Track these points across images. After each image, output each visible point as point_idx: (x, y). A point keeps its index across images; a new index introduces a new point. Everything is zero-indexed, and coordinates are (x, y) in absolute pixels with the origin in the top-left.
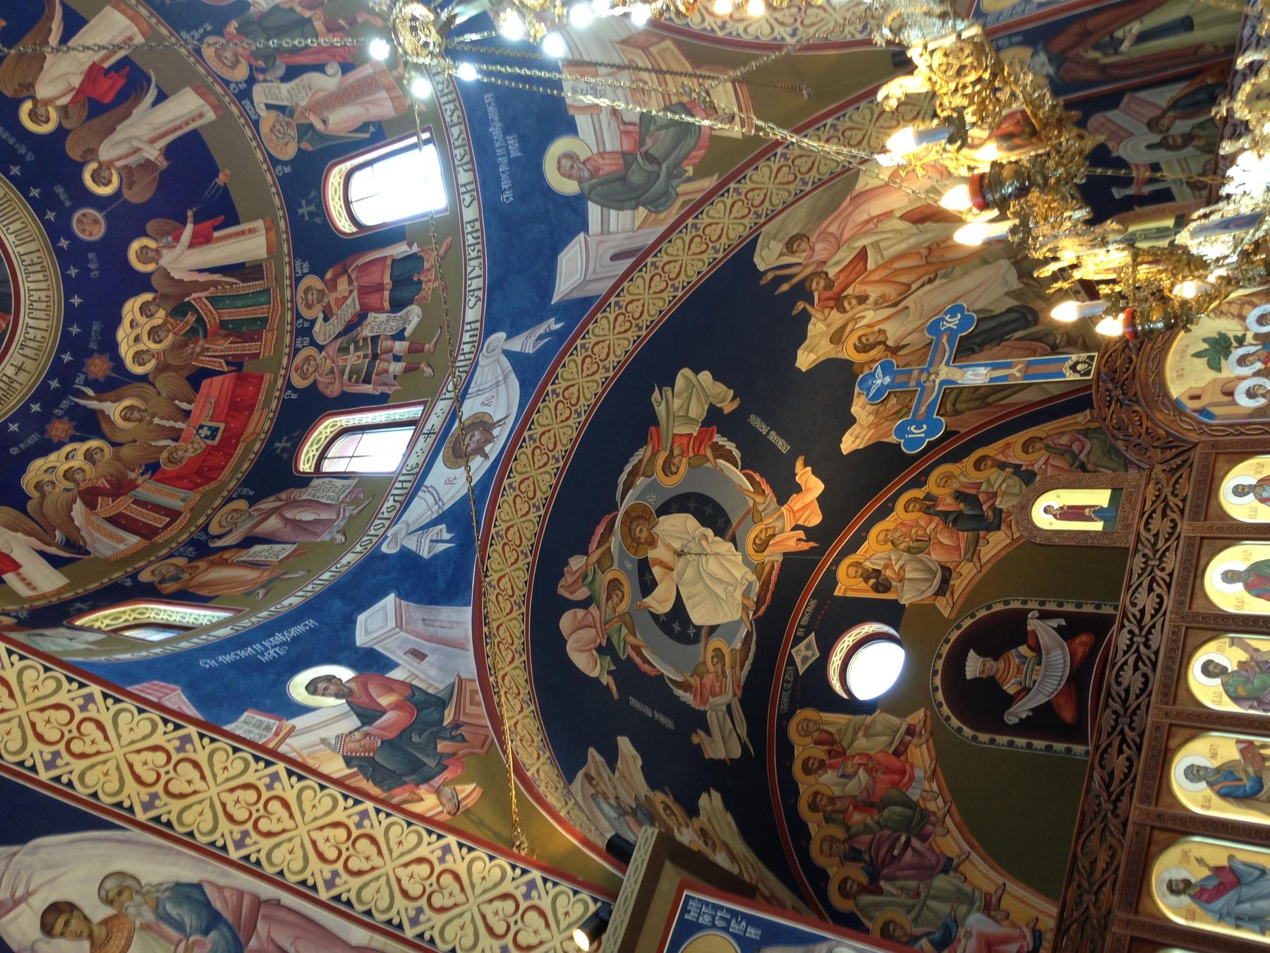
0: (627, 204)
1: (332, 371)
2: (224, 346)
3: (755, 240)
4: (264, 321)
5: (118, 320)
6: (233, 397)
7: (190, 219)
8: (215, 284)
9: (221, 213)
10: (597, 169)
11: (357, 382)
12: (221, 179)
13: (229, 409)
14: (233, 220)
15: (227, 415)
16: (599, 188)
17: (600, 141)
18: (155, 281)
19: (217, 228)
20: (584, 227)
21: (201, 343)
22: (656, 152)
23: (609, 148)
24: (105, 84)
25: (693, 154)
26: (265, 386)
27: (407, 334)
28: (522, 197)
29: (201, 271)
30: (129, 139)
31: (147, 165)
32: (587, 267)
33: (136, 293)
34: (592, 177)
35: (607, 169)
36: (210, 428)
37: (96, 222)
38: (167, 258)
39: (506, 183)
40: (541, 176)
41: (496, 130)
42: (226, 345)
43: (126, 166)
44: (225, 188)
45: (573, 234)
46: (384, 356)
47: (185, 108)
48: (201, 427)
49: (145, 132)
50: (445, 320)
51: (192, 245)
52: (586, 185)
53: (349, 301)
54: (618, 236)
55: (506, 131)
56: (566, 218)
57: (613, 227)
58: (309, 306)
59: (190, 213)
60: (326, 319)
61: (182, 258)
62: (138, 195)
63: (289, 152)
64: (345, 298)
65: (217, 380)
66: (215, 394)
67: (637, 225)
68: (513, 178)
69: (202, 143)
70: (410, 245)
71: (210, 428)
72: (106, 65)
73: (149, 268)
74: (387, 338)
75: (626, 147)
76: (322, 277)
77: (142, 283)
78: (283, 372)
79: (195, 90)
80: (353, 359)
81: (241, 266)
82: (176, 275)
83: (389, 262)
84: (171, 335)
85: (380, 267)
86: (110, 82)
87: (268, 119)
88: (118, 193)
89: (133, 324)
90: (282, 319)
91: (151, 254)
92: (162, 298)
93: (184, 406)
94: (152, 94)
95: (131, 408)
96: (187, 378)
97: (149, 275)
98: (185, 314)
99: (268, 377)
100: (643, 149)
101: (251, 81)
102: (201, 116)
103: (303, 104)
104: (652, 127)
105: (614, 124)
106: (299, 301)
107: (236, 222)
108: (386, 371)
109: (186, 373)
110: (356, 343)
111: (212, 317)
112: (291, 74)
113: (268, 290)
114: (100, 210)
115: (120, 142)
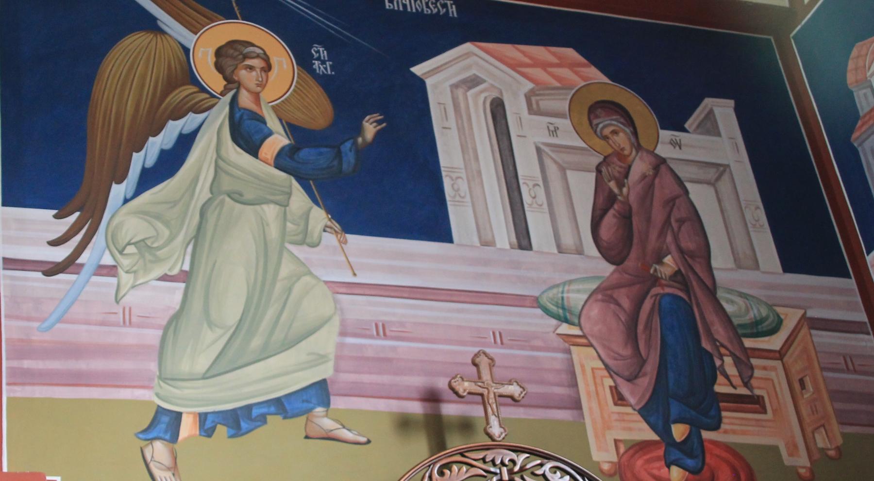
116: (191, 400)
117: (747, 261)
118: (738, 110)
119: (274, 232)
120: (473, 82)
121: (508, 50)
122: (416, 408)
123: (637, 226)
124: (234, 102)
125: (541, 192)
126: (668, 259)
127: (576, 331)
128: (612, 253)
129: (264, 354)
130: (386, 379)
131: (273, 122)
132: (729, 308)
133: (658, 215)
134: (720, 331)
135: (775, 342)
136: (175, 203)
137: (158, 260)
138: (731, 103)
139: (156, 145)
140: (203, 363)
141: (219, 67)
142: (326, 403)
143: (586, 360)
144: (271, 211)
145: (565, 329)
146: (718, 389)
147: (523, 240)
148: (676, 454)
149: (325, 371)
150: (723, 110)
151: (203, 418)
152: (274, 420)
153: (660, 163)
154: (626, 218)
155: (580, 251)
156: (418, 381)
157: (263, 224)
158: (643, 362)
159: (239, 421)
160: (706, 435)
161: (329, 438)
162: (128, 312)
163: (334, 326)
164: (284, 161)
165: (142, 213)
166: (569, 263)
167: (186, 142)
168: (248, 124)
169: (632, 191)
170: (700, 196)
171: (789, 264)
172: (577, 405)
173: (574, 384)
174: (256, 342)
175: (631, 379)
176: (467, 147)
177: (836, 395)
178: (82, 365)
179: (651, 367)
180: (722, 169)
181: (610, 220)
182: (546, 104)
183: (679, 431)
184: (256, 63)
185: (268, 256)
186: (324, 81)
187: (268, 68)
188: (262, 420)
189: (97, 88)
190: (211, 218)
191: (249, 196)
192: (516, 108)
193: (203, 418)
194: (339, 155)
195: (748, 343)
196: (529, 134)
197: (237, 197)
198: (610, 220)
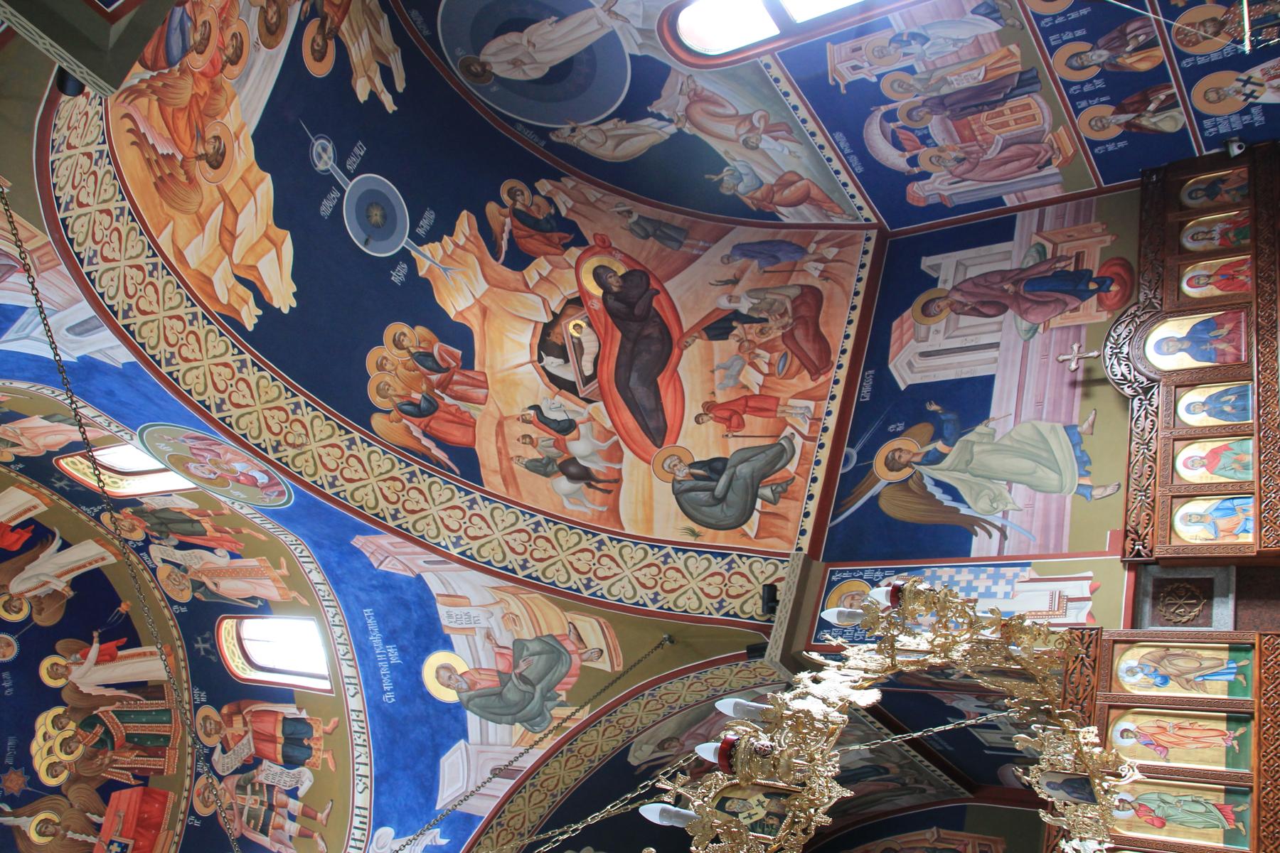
0: (505, 718)
1: (231, 807)
2: (130, 758)
3: (628, 749)
4: (167, 738)
5: (32, 734)
6: (141, 812)
7: (96, 639)
8: (120, 699)
9: (124, 635)
10: (475, 683)
11: (255, 828)
12: (123, 608)
13: (137, 825)
14: (134, 642)
15: (136, 831)
16: (477, 700)
17: (476, 658)
18: (65, 696)
19: (120, 648)
20: (464, 734)
21: (109, 754)
22: (531, 675)
23: (484, 666)
24: (15, 536)
25: (566, 680)
26: (170, 805)
27: (301, 793)
28: (404, 699)
29: (107, 686)
30: (38, 575)
31: (55, 594)
32: (469, 770)
33: (48, 708)
34: (470, 689)
35: (484, 684)
36: (120, 844)
37: (9, 645)
38: (76, 674)
39: (387, 685)
40: (420, 684)
41: (376, 639)
42: (133, 758)
43: (35, 596)
44: (127, 616)
45: (455, 740)
46: (279, 810)
47: (87, 554)
48: (112, 842)
49: (52, 570)
50: (334, 786)
51: (97, 663)
52: (465, 696)
53: (245, 741)
54: (497, 749)
55: (386, 641)
56: (445, 725)
57: (491, 739)
58: (208, 735)
59: (96, 634)
60: (224, 751)
61: (88, 672)
62: (46, 619)
63: (186, 597)
64: (242, 737)
65: (128, 791)
66: (123, 807)
67: (515, 740)
68: (395, 683)
69: (106, 572)
70: (300, 709)
71: (120, 844)
72: (13, 524)
73: (59, 683)
74: (282, 791)
75: (502, 666)
76: (219, 710)
77: (54, 697)
78: (186, 794)
79: (97, 542)
80: (250, 801)
81: (144, 684)
82: (85, 690)
83: (280, 718)
84: (81, 747)
85: (271, 719)
86: (17, 536)
87: (163, 571)
88: (29, 619)
89: (46, 737)
90: (183, 740)
91: (61, 670)
92: (73, 711)
93: (95, 818)
94: (57, 543)
95: (46, 821)
96: (98, 790)
97: (59, 690)
98: (93, 727)
99: (171, 796)
100: (517, 671)
101: (147, 542)
102: (103, 559)
103: (196, 567)
104: (525, 653)
105: (488, 646)
106: (198, 727)
107: (140, 646)
108: (282, 828)
109: (96, 785)
110: (253, 785)
111: (119, 730)
112: (182, 546)
113: (168, 711)
114: (11, 633)
115: (29, 578)
116: (1071, 477)
117: (1008, 256)
118: (928, 255)
119: (988, 447)
120: (910, 365)
121: (893, 350)
122: (1079, 391)
123: (987, 299)
124: (918, 464)
125: (970, 338)
126: (1006, 287)
127: (1042, 326)
128: (1002, 309)
129: (1051, 451)
130: (1064, 402)
131: (930, 447)
132: (1031, 263)
133: (982, 290)
134: (1043, 268)
135: (1049, 247)
136: (971, 488)
137: (1001, 494)
138: (924, 258)
139: (938, 494)
140: (1054, 476)
141: (899, 470)
142: (1076, 426)
143: (1056, 322)
144: (976, 449)
145: (1041, 329)
146: (1072, 269)
147: (995, 345)
148: (1104, 287)
149: (1060, 427)
150: (927, 263)
151: (1081, 476)
152: (1083, 447)
153: (955, 288)
154: (983, 304)
155: (1001, 323)
156: (1066, 390)
157: (983, 452)
158: (1057, 300)
159: (1083, 462)
160: (1095, 275)
161: (1092, 425)
162: (1027, 506)
163: (1037, 423)
164: (951, 444)
165: (976, 501)
166: (1009, 327)
167: (938, 483)
168: (930, 457)
169: (970, 301)
170: (973, 272)
171: (1009, 237)
172: (1079, 327)
173: (1068, 327)
174: (1045, 454)
175: (1066, 304)
176: (945, 367)
177: (1076, 222)
178: (1053, 523)
179: (1060, 296)
180: (958, 264)
181: (984, 310)
182: (923, 334)
183: (1093, 286)
184: (897, 455)
185: (1000, 449)
186: (908, 426)
187: (900, 450)
188: (1083, 452)
189: (908, 520)
190: (980, 473)
191: (968, 457)
192: (924, 347)
193: (1081, 476)
194: (948, 421)
195: (1049, 256)
196: (937, 341)
197: (968, 463)
198: (984, 310)
